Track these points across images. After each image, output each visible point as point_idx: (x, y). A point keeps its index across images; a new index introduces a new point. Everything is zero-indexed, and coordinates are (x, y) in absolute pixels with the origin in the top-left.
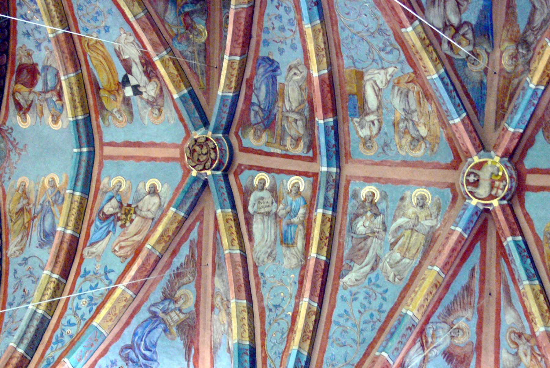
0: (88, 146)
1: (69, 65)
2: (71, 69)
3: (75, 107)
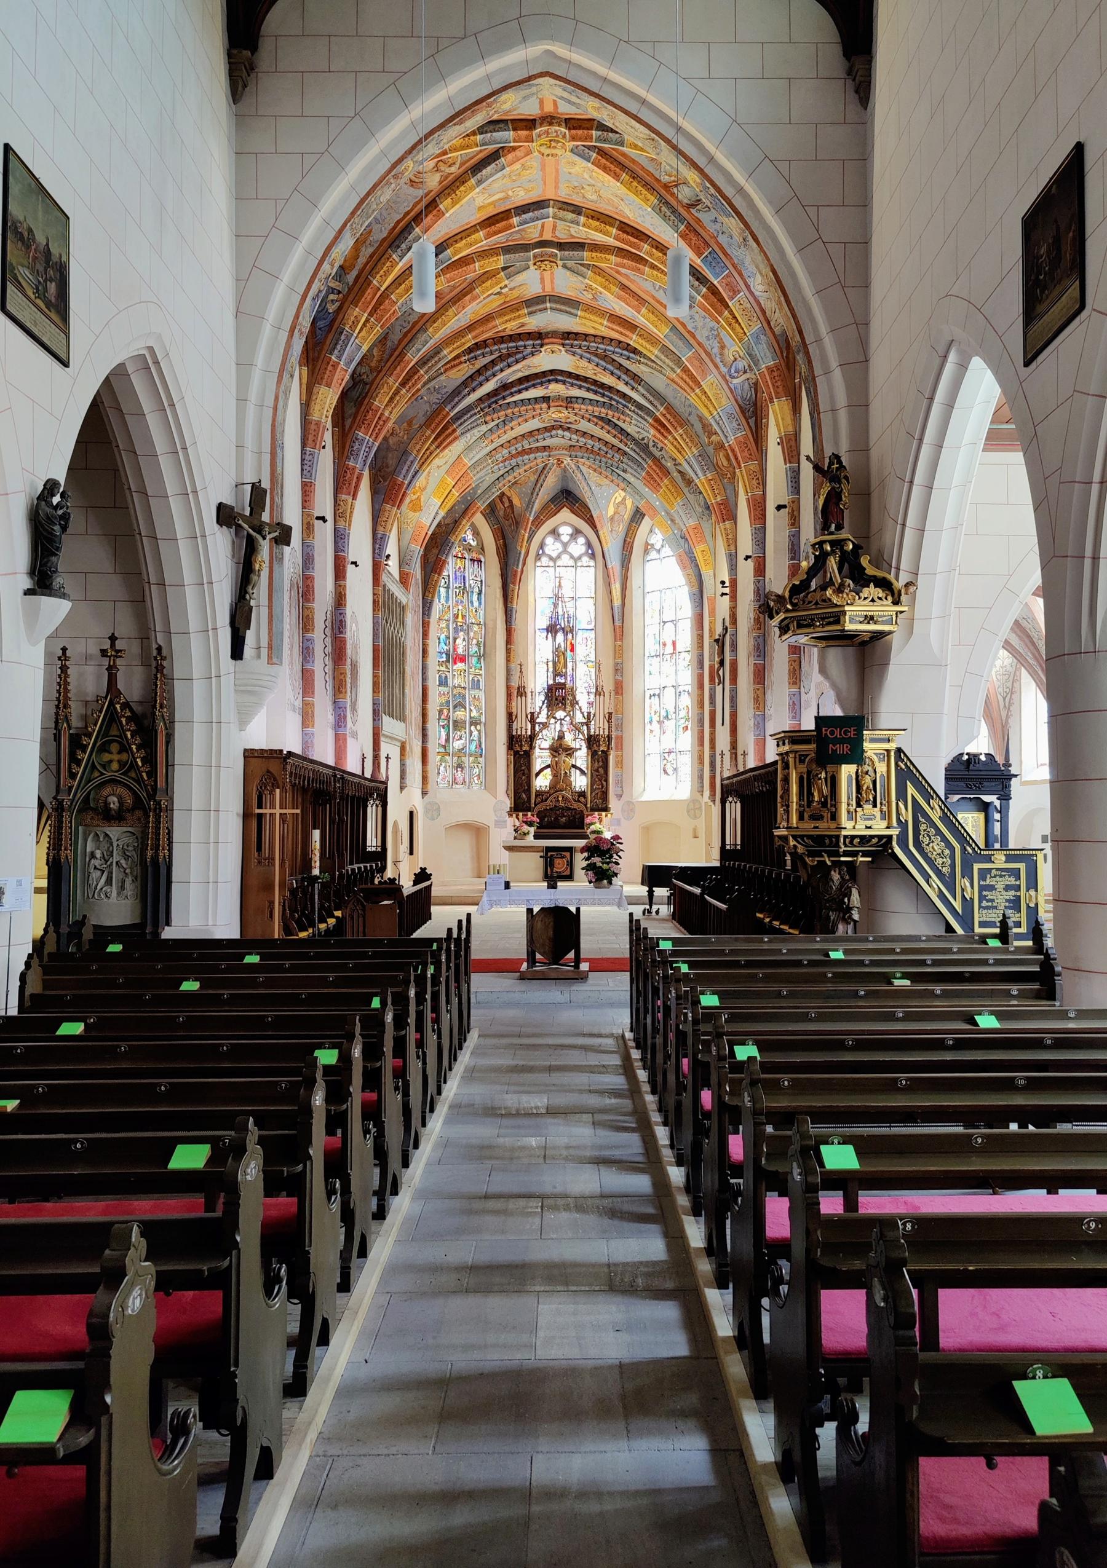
0: (545, 302)
1: (490, 325)
2: (493, 324)
3: (519, 317)
